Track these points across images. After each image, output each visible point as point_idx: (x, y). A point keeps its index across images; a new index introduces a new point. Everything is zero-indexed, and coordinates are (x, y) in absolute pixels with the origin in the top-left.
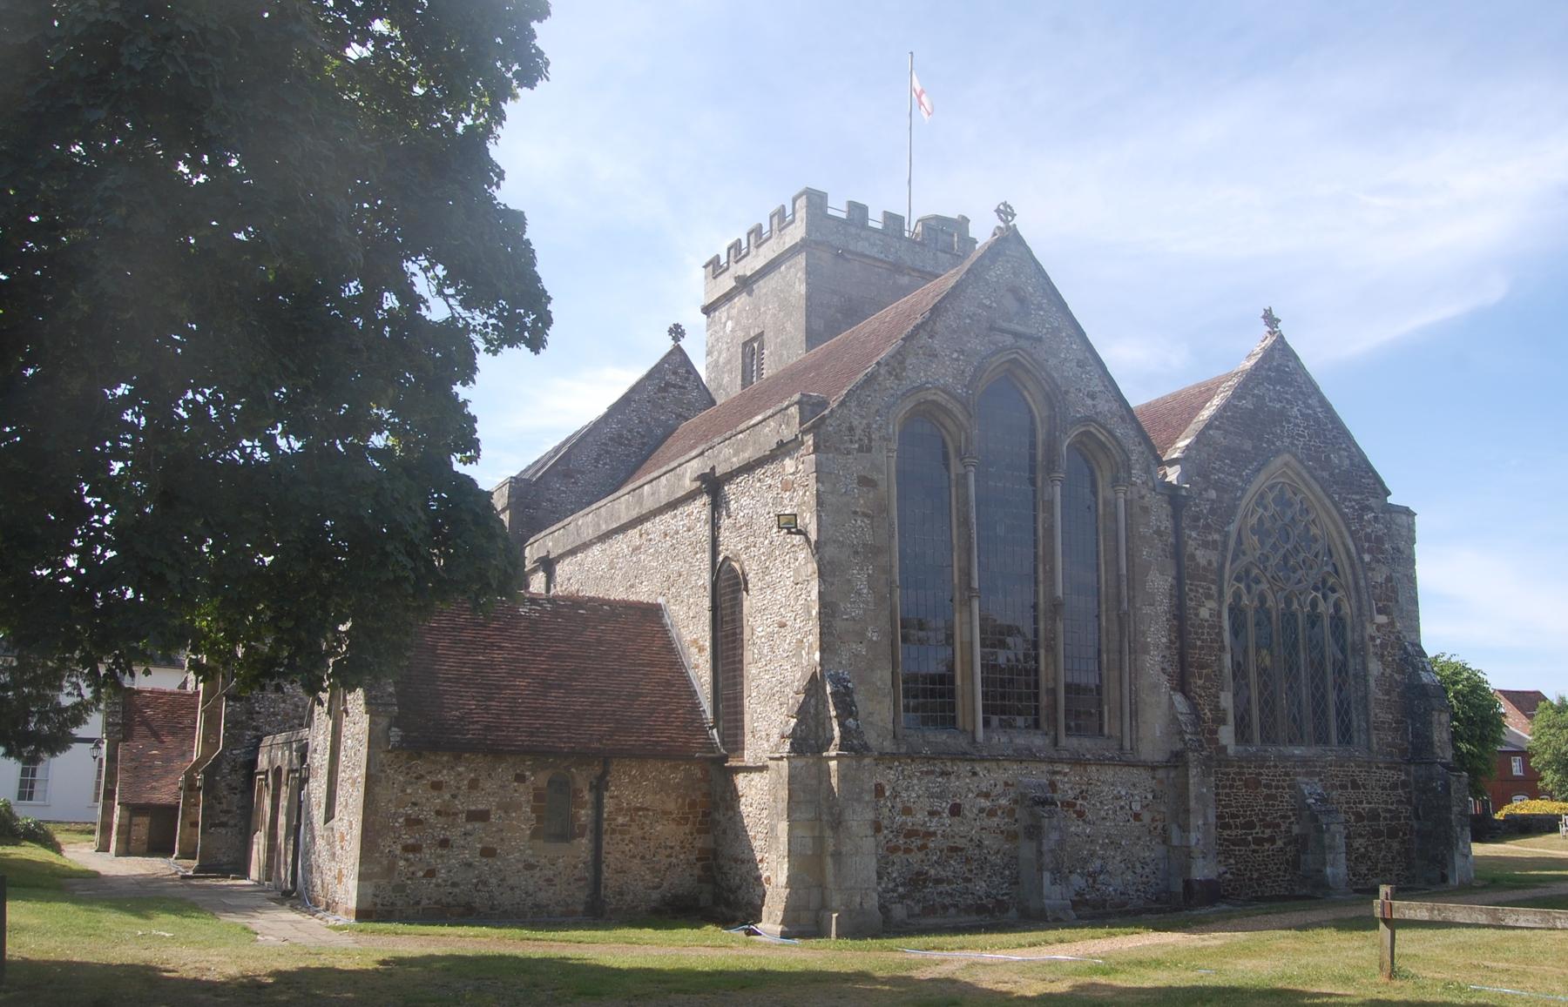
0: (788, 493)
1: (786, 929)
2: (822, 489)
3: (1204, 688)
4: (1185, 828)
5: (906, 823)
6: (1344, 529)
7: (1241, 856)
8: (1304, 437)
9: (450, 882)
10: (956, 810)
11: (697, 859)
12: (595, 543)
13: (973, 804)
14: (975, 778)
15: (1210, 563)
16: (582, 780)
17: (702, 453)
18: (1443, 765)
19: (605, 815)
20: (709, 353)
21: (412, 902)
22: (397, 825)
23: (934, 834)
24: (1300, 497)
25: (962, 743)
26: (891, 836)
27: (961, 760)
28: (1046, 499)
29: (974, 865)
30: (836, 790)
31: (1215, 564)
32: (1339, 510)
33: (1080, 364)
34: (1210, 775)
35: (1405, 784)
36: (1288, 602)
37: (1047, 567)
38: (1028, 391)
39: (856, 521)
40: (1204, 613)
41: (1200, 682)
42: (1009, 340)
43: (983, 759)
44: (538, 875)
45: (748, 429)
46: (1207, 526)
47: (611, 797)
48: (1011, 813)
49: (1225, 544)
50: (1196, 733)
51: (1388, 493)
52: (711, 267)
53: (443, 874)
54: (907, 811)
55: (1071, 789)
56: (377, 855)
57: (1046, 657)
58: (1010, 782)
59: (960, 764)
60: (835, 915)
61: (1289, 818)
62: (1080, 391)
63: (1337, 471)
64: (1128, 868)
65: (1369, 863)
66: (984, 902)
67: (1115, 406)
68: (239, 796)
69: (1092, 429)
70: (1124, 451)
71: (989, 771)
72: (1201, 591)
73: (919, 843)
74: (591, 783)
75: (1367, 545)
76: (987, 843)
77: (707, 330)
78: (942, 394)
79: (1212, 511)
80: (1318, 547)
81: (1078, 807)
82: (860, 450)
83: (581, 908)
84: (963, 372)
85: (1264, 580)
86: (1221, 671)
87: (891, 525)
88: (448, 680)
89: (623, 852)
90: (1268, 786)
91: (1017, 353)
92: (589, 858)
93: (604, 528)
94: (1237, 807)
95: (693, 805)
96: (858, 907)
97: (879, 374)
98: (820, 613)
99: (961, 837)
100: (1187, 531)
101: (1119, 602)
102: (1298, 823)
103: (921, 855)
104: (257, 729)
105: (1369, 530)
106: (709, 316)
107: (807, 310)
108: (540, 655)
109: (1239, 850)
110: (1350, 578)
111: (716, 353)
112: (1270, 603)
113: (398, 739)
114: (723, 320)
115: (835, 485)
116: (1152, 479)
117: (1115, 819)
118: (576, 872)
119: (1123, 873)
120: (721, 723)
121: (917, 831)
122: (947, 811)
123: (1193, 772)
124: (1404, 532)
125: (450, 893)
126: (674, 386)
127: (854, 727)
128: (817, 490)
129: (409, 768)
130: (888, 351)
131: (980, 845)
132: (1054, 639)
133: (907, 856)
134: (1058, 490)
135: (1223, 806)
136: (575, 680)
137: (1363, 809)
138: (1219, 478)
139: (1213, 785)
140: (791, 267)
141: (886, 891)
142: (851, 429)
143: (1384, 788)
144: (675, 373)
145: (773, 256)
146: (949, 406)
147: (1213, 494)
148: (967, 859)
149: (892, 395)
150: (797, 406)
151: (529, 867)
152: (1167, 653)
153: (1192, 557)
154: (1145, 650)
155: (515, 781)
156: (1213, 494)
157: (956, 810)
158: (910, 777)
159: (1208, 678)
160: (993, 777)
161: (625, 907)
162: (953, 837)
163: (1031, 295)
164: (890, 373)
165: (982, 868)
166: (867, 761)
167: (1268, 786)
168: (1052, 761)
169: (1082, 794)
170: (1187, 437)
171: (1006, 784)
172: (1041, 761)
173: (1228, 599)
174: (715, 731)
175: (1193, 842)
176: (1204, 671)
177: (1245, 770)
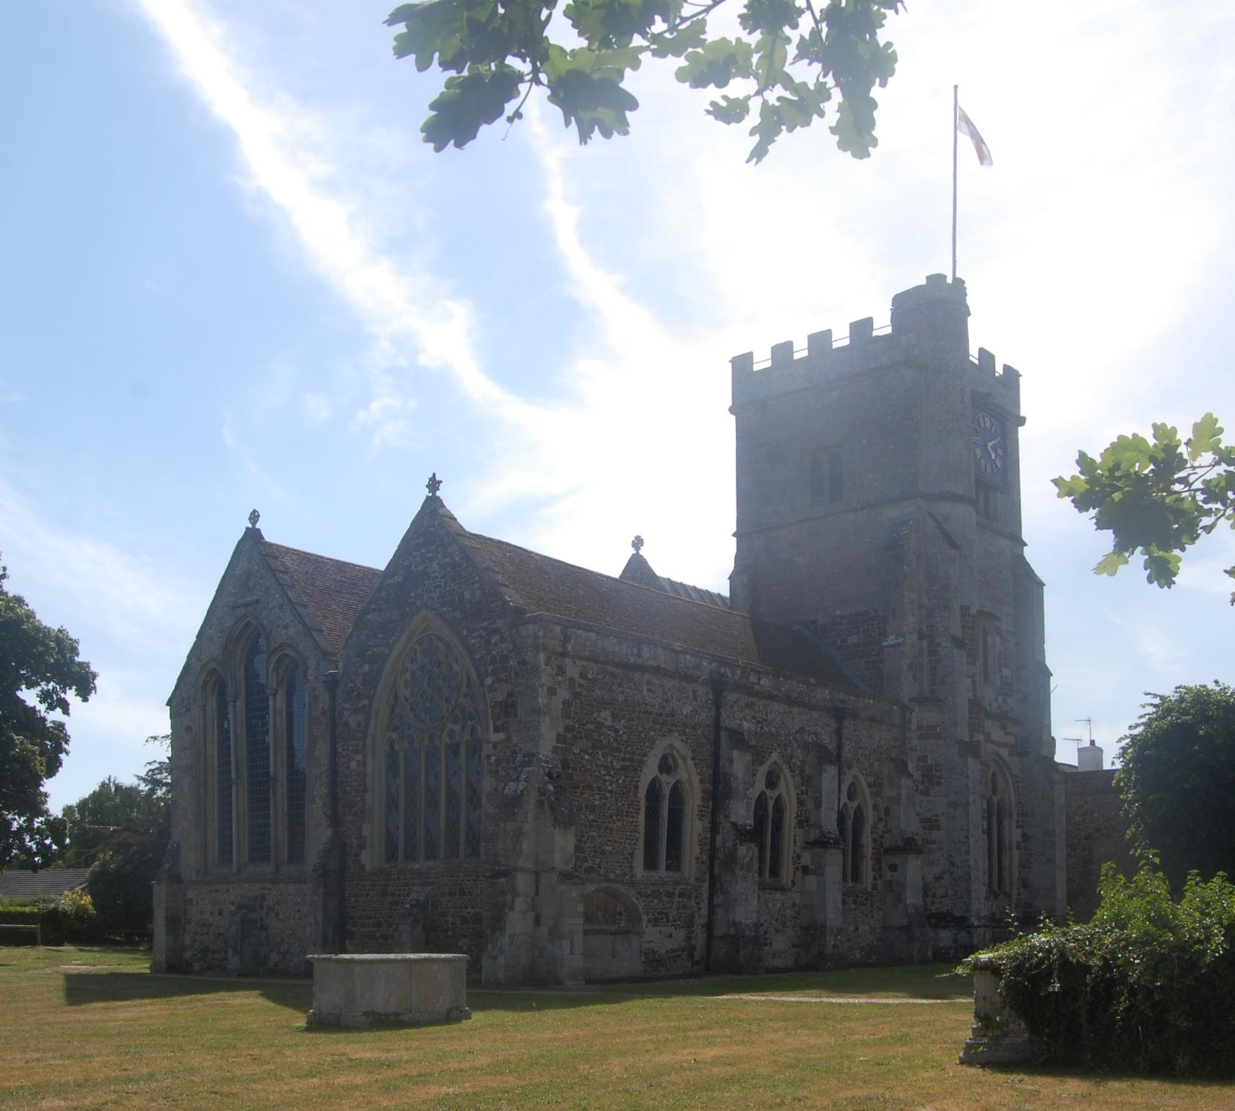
15: (359, 725)
23: (212, 925)
41: (349, 818)
54: (201, 913)
63: (468, 606)
69: (285, 651)
75: (490, 669)
82: (186, 711)
90: (393, 894)
137: (468, 913)
138: (373, 652)
147: (366, 668)
153: (347, 724)
157: (221, 912)
176: (352, 810)
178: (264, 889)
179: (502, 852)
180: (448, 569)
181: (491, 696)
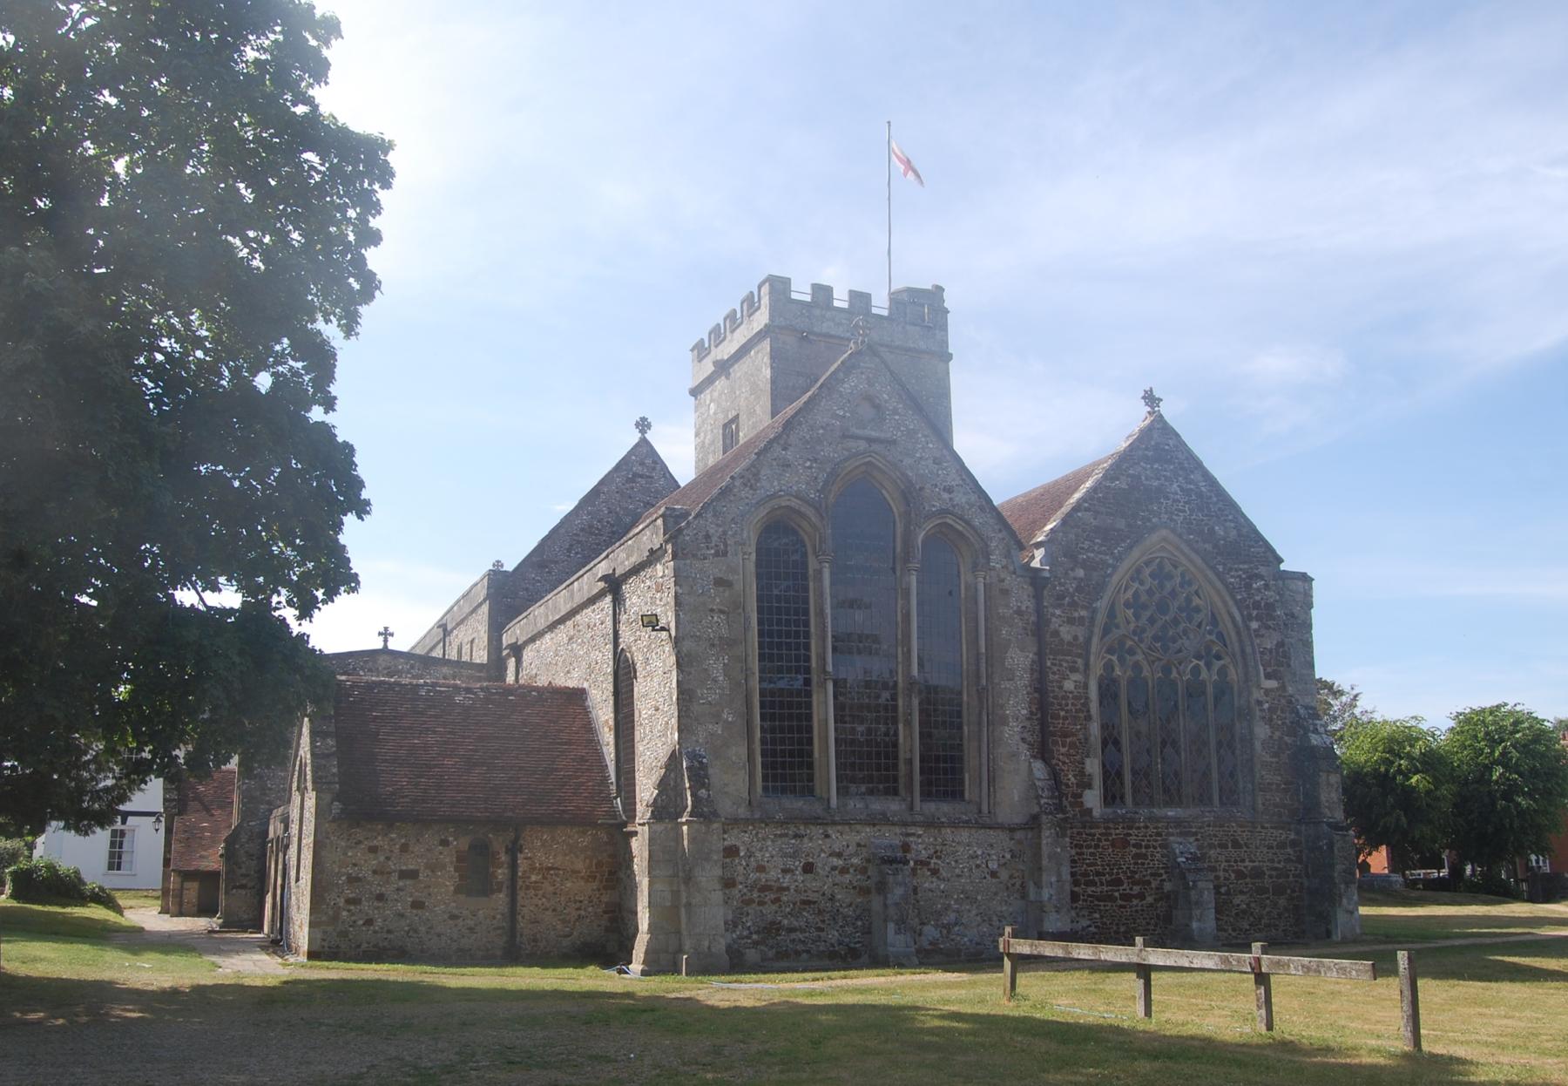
0: (659, 594)
1: (646, 968)
2: (680, 591)
3: (1068, 755)
4: (1038, 885)
5: (760, 880)
6: (1228, 598)
7: (1107, 910)
8: (1185, 511)
9: (386, 929)
10: (808, 868)
11: (605, 912)
12: (547, 632)
13: (823, 862)
14: (827, 840)
15: (1076, 638)
16: (499, 844)
17: (607, 556)
18: (1329, 824)
19: (520, 874)
20: (697, 435)
21: (353, 946)
22: (340, 882)
23: (788, 889)
24: (1180, 569)
25: (818, 809)
26: (745, 890)
27: (813, 824)
28: (904, 587)
29: (827, 917)
30: (687, 851)
31: (1081, 639)
32: (1223, 581)
33: (937, 461)
34: (1064, 835)
35: (1294, 844)
36: (1167, 670)
37: (905, 649)
38: (886, 489)
39: (713, 617)
40: (1069, 685)
41: (1063, 750)
42: (862, 445)
43: (834, 823)
44: (461, 924)
45: (634, 536)
46: (1073, 605)
47: (526, 859)
48: (863, 871)
49: (1092, 620)
50: (1051, 798)
51: (1280, 560)
52: (696, 352)
53: (379, 922)
55: (925, 849)
56: (324, 906)
57: (904, 730)
58: (863, 844)
59: (812, 827)
60: (685, 957)
61: (1161, 875)
62: (936, 486)
63: (1222, 542)
64: (984, 921)
65: (1252, 919)
66: (837, 949)
67: (973, 498)
68: (255, 862)
70: (982, 539)
71: (841, 834)
72: (1065, 664)
73: (773, 896)
74: (507, 846)
75: (1255, 613)
76: (839, 897)
77: (696, 412)
78: (795, 500)
79: (1079, 589)
80: (1198, 618)
81: (932, 866)
82: (717, 554)
83: (499, 953)
84: (816, 478)
85: (1139, 651)
86: (1086, 739)
87: (747, 619)
88: (386, 761)
89: (537, 905)
91: (870, 456)
92: (506, 910)
93: (552, 618)
94: (1102, 865)
95: (599, 864)
96: (706, 950)
97: (735, 486)
98: (678, 699)
99: (814, 891)
100: (1051, 610)
101: (978, 677)
102: (1170, 880)
103: (774, 907)
104: (269, 803)
105: (1258, 598)
106: (696, 399)
107: (772, 394)
108: (469, 737)
109: (1105, 906)
110: (1236, 645)
111: (702, 434)
112: (1146, 673)
113: (338, 811)
114: (708, 402)
115: (692, 588)
116: (1013, 562)
117: (970, 876)
118: (495, 922)
119: (979, 925)
120: (623, 794)
121: (771, 886)
122: (799, 868)
123: (1046, 833)
124: (1299, 598)
125: (386, 939)
126: (641, 476)
127: (706, 796)
128: (676, 593)
129: (350, 835)
130: (744, 464)
131: (832, 899)
132: (910, 714)
133: (761, 908)
134: (914, 579)
135: (1088, 865)
136: (498, 758)
137: (1245, 867)
138: (1088, 557)
139: (1068, 845)
140: (758, 352)
141: (741, 937)
142: (708, 537)
143: (1270, 847)
144: (642, 464)
145: (744, 340)
146: (803, 509)
147: (1080, 573)
148: (819, 910)
149: (747, 504)
150: (661, 519)
151: (453, 917)
152: (1027, 724)
153: (1056, 633)
154: (1004, 721)
155: (441, 845)
156: (1080, 573)
157: (808, 868)
158: (764, 840)
159: (1072, 746)
160: (843, 839)
161: (539, 952)
162: (805, 891)
163: (886, 401)
164: (745, 485)
165: (834, 919)
166: (715, 826)
167: (1134, 846)
168: (905, 824)
169: (937, 854)
170: (1055, 521)
171: (859, 845)
172: (893, 824)
173: (1097, 670)
174: (619, 799)
175: (1046, 896)
176: (1068, 740)
177: (1113, 831)
178: (908, 835)
179: (1327, 804)
180: (1194, 497)
181: (1258, 641)
